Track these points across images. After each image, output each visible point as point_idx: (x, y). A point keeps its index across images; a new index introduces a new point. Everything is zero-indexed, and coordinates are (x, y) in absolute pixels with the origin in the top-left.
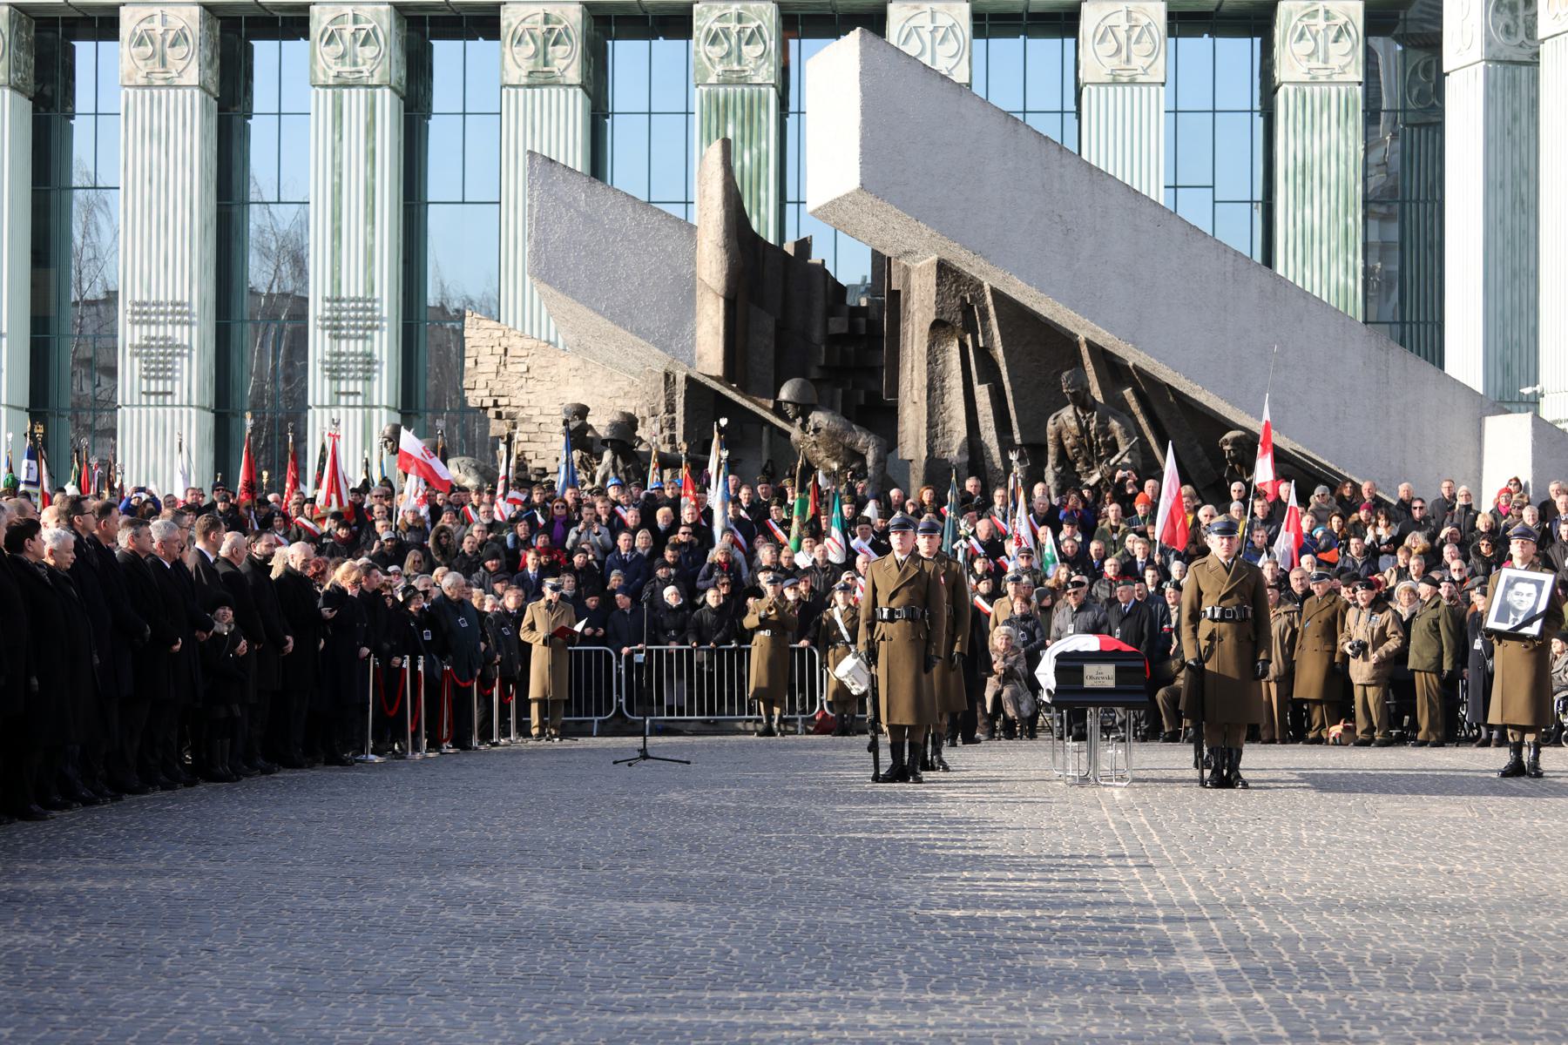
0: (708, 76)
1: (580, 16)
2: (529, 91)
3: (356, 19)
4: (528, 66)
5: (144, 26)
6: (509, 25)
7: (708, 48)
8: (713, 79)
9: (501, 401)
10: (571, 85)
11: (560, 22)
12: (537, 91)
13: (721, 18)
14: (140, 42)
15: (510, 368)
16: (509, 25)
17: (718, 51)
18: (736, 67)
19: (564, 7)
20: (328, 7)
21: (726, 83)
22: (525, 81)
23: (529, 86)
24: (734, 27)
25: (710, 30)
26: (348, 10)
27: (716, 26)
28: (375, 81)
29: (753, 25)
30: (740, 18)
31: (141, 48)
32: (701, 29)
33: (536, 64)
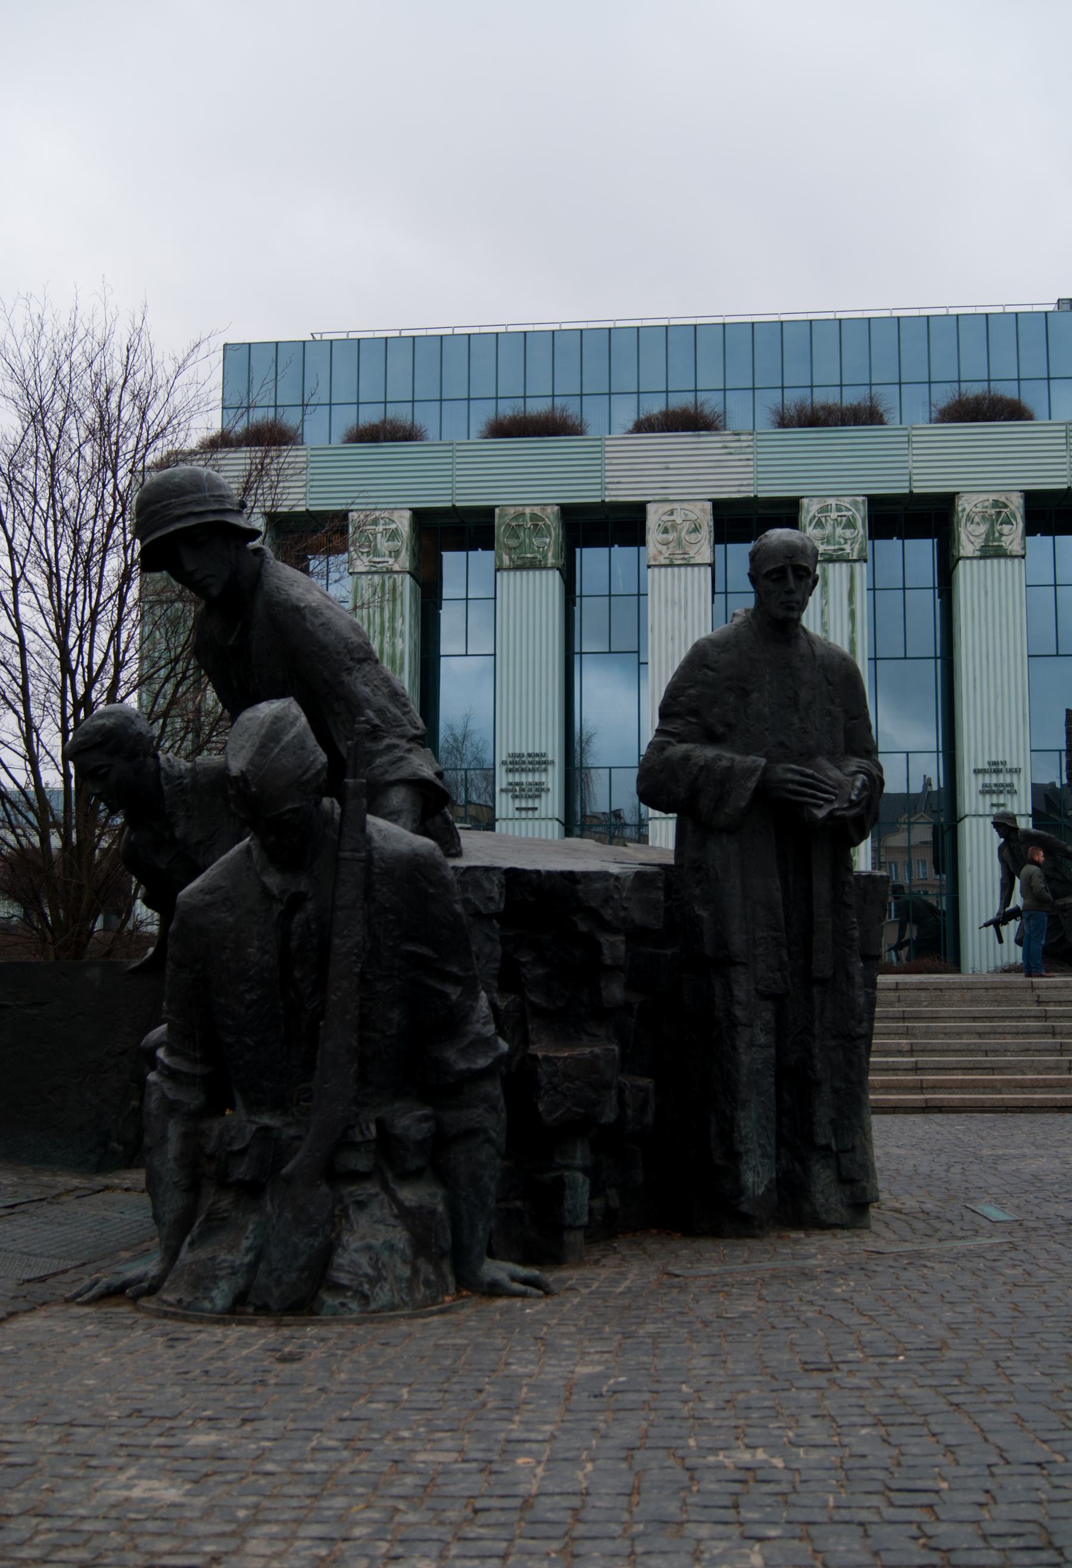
2: (982, 561)
3: (839, 509)
4: (979, 542)
5: (666, 518)
6: (964, 510)
11: (1006, 506)
12: (989, 561)
14: (666, 531)
16: (964, 510)
19: (1008, 495)
20: (815, 499)
22: (978, 554)
23: (980, 558)
26: (832, 501)
28: (855, 557)
31: (665, 536)
33: (987, 539)
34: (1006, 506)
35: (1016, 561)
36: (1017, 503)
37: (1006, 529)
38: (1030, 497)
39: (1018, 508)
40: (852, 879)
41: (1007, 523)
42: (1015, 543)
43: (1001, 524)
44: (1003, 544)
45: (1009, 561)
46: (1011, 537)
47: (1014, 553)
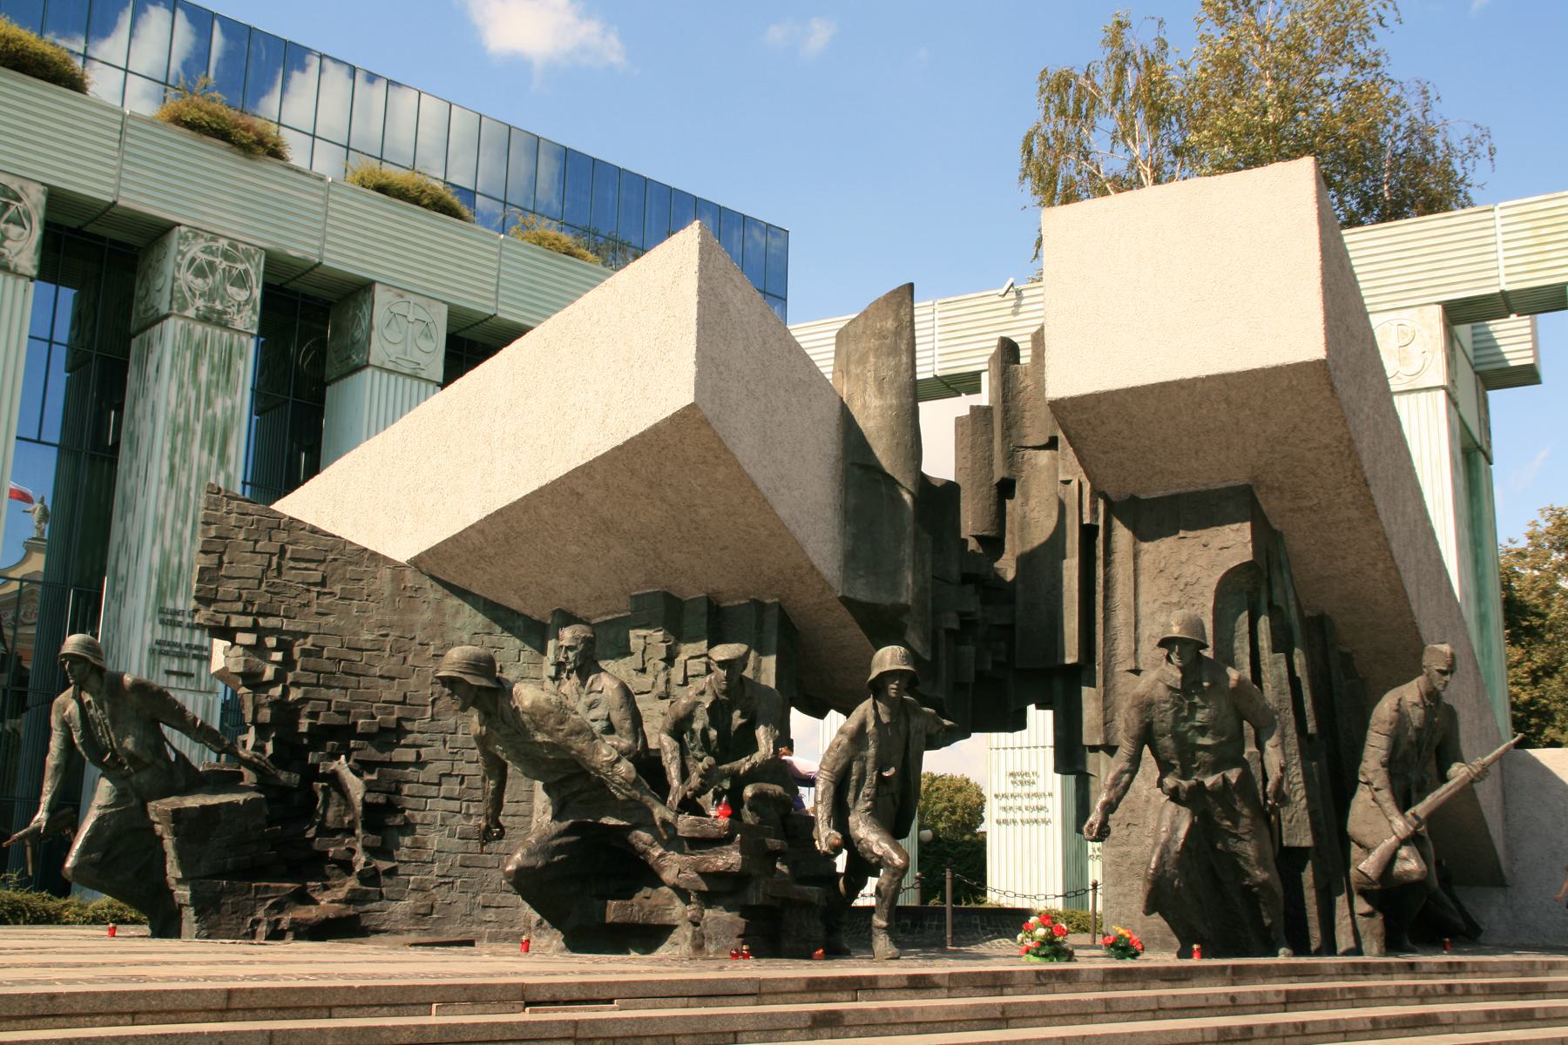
0: (184, 307)
1: (43, 199)
7: (190, 277)
8: (191, 313)
9: (261, 621)
10: (22, 275)
11: (19, 199)
13: (205, 250)
15: (288, 575)
17: (200, 281)
18: (219, 307)
19: (25, 184)
21: (204, 319)
24: (222, 264)
25: (193, 260)
27: (203, 258)
29: (241, 267)
30: (226, 256)
32: (184, 255)
34: (19, 199)
35: (22, 282)
36: (34, 201)
37: (14, 230)
38: (56, 199)
39: (36, 206)
40: (913, 637)
41: (15, 223)
42: (23, 255)
43: (8, 221)
44: (6, 252)
45: (10, 279)
46: (19, 245)
47: (20, 270)
